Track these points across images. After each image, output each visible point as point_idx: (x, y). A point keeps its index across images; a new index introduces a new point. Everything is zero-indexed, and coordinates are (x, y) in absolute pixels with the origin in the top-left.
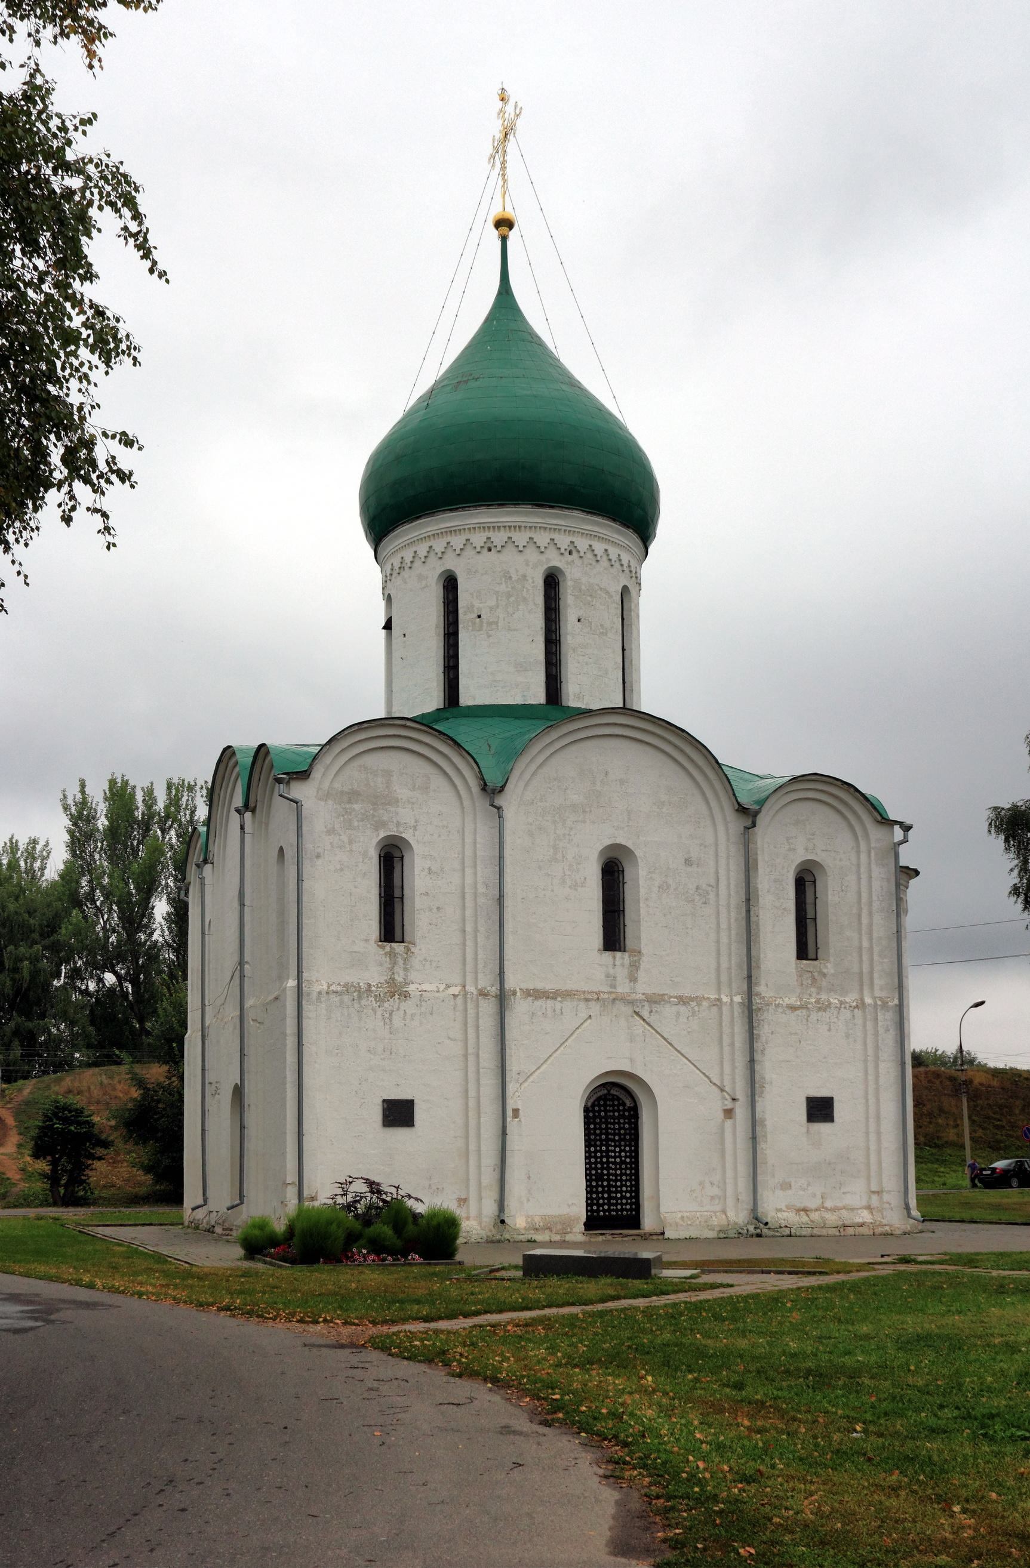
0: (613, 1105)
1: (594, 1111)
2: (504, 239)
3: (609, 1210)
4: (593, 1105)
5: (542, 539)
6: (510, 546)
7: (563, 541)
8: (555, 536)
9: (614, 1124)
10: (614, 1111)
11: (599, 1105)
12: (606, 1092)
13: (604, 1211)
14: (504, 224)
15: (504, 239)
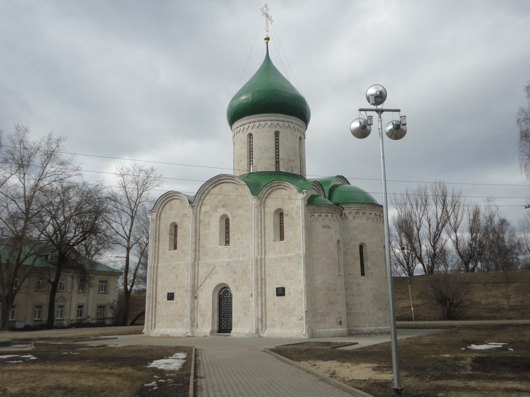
0: (228, 294)
1: (222, 296)
2: (267, 43)
3: (225, 327)
4: (222, 294)
5: (246, 126)
6: (278, 126)
7: (251, 125)
8: (249, 124)
9: (228, 299)
10: (228, 295)
11: (224, 294)
12: (226, 290)
13: (224, 327)
14: (267, 39)
15: (267, 43)
